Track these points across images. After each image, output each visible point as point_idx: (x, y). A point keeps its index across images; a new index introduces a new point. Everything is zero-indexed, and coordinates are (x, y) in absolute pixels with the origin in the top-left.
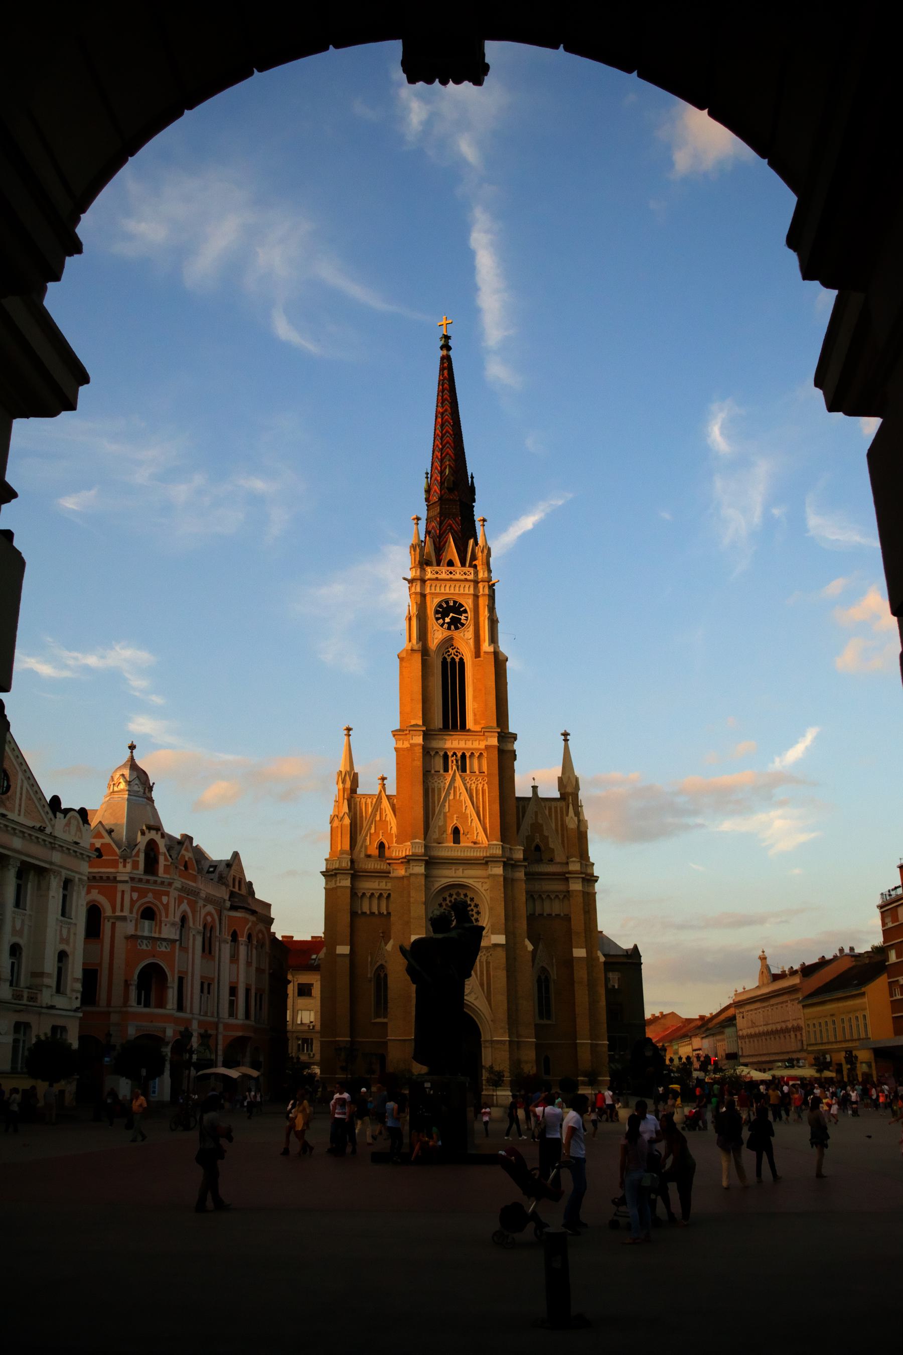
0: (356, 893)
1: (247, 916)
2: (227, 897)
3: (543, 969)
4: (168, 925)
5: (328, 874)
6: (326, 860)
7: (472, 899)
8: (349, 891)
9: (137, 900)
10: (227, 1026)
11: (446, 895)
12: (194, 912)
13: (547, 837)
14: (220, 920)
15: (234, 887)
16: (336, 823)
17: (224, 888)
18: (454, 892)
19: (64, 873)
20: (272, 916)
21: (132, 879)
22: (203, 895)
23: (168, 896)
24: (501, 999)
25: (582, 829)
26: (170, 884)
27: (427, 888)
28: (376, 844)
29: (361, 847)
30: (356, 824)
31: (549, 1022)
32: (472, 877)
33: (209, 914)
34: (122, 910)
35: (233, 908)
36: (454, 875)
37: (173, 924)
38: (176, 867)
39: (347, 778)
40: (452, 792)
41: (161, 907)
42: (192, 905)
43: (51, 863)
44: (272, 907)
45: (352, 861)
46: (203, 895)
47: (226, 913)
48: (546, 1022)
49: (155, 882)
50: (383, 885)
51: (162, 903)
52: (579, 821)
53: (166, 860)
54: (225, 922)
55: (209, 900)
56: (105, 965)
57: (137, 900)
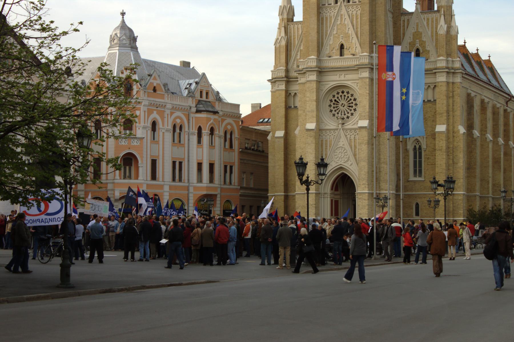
2: (194, 105)
3: (417, 141)
4: (141, 129)
5: (273, 81)
6: (272, 71)
7: (352, 95)
8: (283, 93)
10: (195, 188)
11: (335, 93)
12: (163, 118)
13: (425, 42)
14: (188, 120)
15: (201, 97)
18: (340, 91)
20: (241, 113)
23: (140, 110)
24: (364, 165)
25: (453, 33)
27: (318, 90)
29: (294, 61)
31: (420, 179)
32: (348, 79)
33: (178, 117)
35: (198, 111)
36: (338, 79)
37: (144, 128)
39: (285, 11)
40: (339, 18)
42: (161, 114)
44: (241, 107)
45: (287, 71)
46: (169, 106)
47: (192, 115)
48: (418, 179)
52: (449, 27)
54: (193, 122)
55: (174, 109)
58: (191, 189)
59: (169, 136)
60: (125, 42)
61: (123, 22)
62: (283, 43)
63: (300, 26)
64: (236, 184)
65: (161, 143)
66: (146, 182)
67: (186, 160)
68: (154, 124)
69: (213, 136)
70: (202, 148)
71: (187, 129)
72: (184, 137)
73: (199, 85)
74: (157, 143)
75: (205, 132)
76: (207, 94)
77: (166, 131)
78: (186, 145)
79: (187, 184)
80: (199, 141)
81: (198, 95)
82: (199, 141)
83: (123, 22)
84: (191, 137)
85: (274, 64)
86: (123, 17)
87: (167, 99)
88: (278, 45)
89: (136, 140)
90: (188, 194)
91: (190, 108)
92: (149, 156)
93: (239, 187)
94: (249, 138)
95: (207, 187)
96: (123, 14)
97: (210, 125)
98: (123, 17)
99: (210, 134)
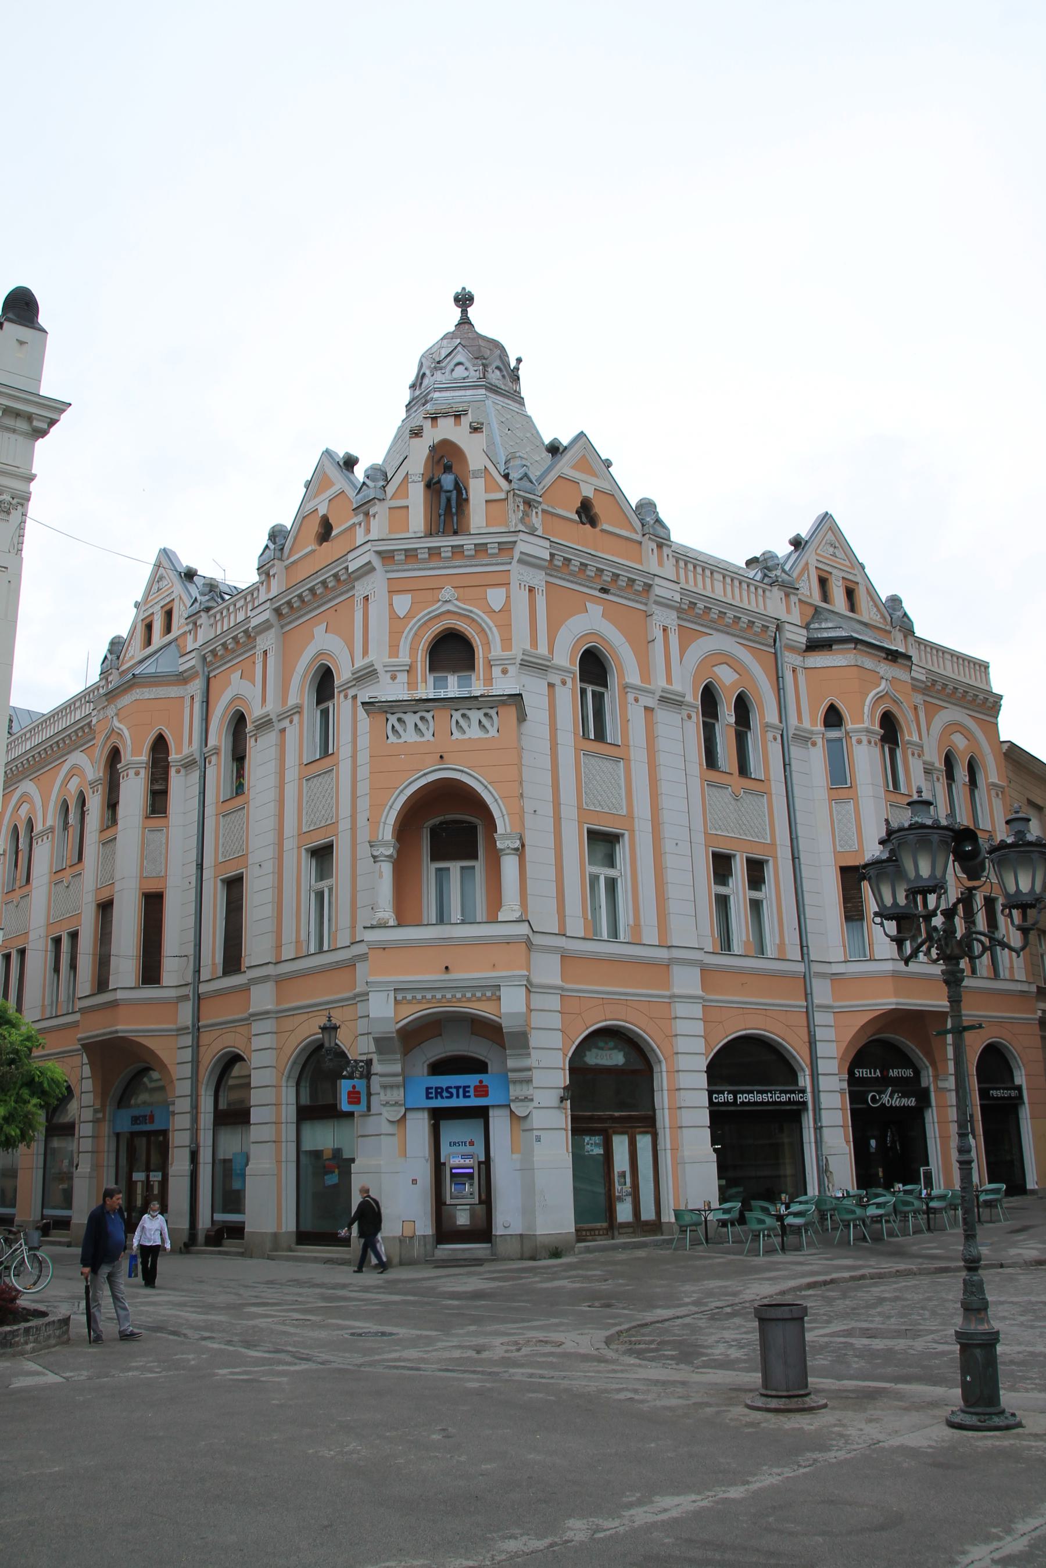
1: (868, 663)
4: (512, 670)
9: (408, 617)
17: (776, 593)
20: (996, 689)
21: (386, 556)
26: (506, 548)
34: (365, 652)
35: (815, 646)
38: (528, 503)
41: (487, 621)
44: (992, 670)
47: (791, 659)
49: (457, 551)
53: (491, 485)
56: (344, 825)
58: (822, 993)
59: (681, 735)
60: (466, 374)
61: (465, 321)
64: (1020, 975)
66: (561, 942)
67: (784, 853)
68: (594, 666)
69: (899, 753)
70: (856, 800)
73: (810, 549)
74: (620, 756)
76: (850, 593)
77: (663, 700)
78: (778, 788)
79: (801, 968)
80: (839, 775)
81: (810, 590)
82: (839, 775)
83: (465, 321)
84: (795, 751)
86: (464, 312)
87: (654, 559)
89: (475, 715)
90: (808, 1014)
91: (778, 628)
93: (1033, 989)
94: (1039, 802)
95: (895, 975)
96: (464, 300)
97: (879, 699)
98: (464, 312)
99: (884, 739)
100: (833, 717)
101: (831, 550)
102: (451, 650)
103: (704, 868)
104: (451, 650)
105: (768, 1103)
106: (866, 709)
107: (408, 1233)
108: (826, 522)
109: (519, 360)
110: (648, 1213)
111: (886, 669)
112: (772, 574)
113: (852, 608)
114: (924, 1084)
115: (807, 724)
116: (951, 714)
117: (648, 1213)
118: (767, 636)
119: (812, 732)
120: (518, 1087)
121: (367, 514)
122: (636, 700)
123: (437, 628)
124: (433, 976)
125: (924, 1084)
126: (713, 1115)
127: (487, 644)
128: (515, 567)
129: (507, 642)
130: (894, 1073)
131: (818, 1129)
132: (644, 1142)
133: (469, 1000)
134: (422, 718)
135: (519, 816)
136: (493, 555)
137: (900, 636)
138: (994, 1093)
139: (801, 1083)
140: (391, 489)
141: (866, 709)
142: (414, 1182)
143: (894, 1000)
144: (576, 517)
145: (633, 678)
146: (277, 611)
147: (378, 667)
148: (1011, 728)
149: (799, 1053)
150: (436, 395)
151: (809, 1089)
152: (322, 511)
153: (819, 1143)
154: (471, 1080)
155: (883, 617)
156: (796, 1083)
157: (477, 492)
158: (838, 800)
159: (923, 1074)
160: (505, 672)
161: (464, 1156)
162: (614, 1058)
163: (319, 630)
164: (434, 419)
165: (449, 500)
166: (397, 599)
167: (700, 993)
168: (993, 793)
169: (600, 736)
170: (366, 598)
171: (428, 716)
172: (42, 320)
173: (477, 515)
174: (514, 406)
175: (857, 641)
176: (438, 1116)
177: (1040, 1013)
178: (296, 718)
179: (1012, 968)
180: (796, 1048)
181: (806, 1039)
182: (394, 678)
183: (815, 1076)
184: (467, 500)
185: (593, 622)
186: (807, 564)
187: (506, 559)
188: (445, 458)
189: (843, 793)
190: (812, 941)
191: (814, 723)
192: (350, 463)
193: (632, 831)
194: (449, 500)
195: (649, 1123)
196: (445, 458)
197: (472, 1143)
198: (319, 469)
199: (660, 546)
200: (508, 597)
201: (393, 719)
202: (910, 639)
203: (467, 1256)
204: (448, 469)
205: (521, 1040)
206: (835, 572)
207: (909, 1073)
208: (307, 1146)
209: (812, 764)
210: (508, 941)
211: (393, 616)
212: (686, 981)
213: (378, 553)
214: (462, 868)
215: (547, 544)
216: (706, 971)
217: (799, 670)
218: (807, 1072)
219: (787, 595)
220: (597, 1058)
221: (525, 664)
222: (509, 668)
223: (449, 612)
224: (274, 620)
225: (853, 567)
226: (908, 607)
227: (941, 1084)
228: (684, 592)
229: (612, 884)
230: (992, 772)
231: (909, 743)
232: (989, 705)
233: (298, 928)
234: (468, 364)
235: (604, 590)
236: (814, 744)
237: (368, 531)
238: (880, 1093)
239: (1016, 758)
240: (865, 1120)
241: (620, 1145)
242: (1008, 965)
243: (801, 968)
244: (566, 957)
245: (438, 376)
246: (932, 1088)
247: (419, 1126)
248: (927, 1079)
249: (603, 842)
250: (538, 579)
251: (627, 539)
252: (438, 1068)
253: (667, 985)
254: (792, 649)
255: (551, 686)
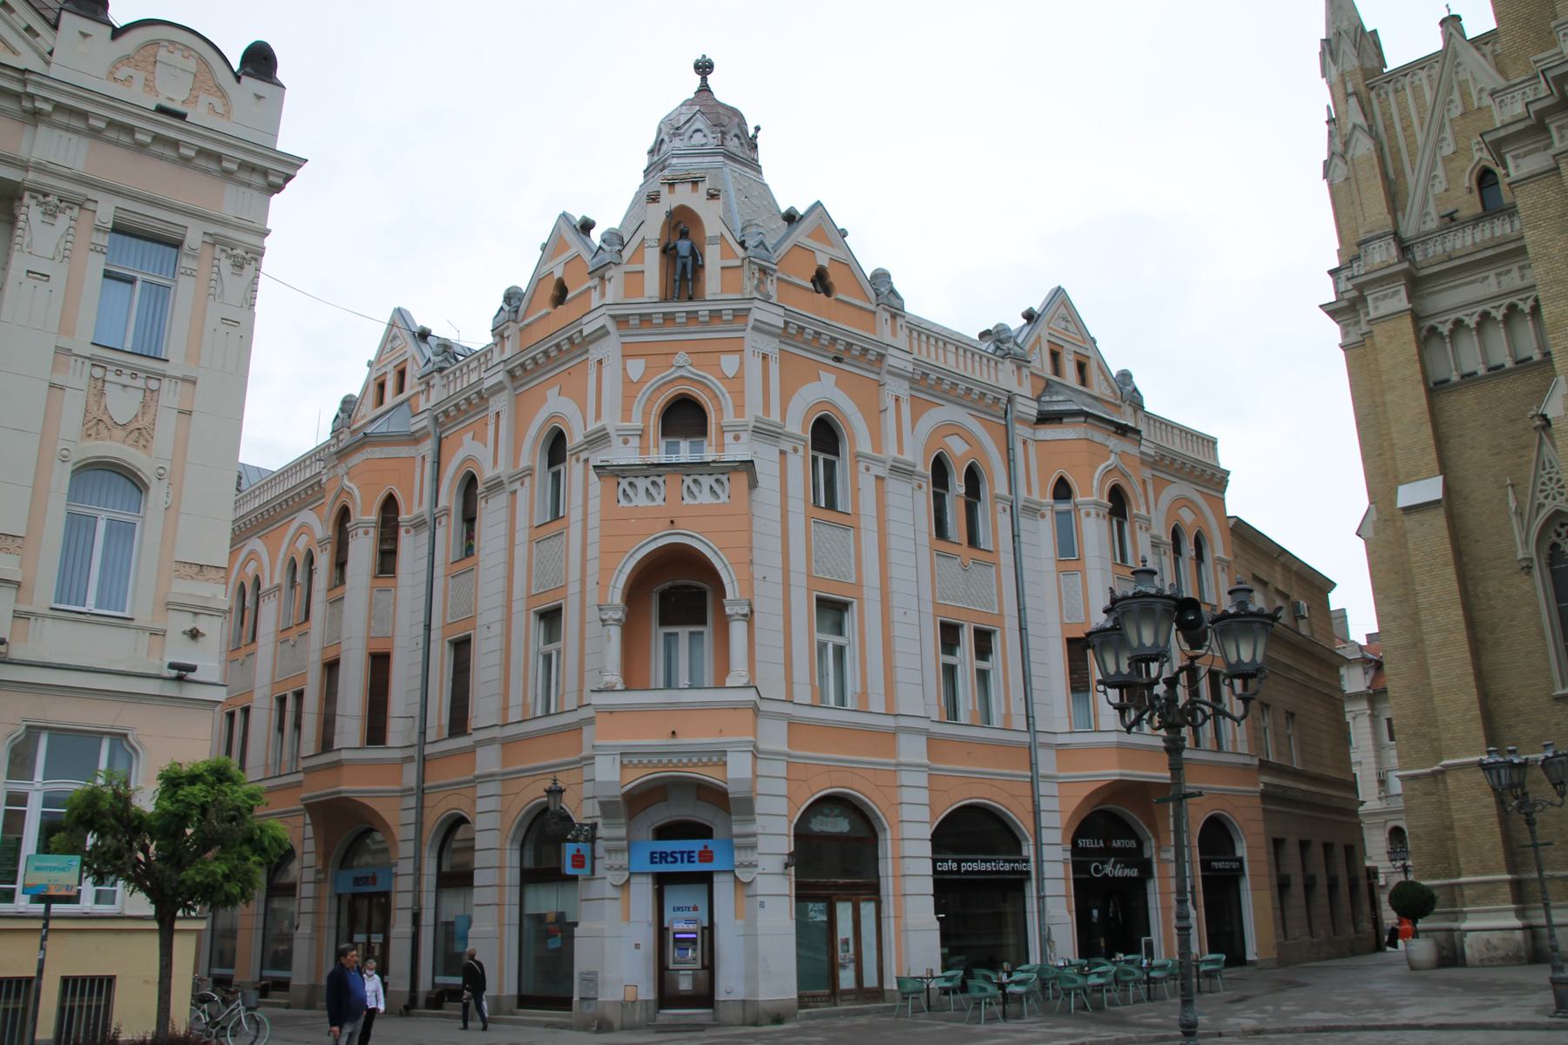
0: (1433, 330)
1: (1098, 436)
4: (744, 436)
6: (1332, 273)
9: (641, 382)
16: (1341, 170)
17: (1008, 366)
19: (107, 210)
21: (621, 321)
22: (894, 360)
26: (740, 315)
28: (1468, 180)
30: (1396, 152)
34: (598, 416)
35: (1045, 418)
38: (764, 271)
41: (720, 387)
43: (41, 168)
47: (1021, 431)
49: (692, 316)
50: (1514, 280)
51: (723, 378)
53: (727, 252)
56: (574, 588)
57: (641, 382)
58: (1047, 763)
59: (911, 505)
60: (704, 141)
61: (704, 89)
62: (1363, 146)
63: (1423, 74)
64: (1243, 748)
65: (869, 524)
66: (787, 708)
67: (1011, 624)
68: (826, 434)
69: (1127, 526)
70: (1083, 572)
71: (1002, 488)
72: (994, 524)
73: (1042, 323)
74: (850, 525)
75: (1091, 495)
76: (1081, 368)
77: (894, 469)
78: (1006, 559)
79: (1026, 738)
80: (1067, 547)
82: (1067, 547)
83: (704, 89)
84: (1025, 523)
85: (1337, 246)
86: (704, 79)
87: (887, 329)
88: (1341, 170)
89: (707, 481)
91: (1010, 400)
92: (799, 580)
93: (1256, 762)
94: (1264, 577)
95: (1120, 746)
96: (704, 68)
97: (1108, 472)
98: (704, 79)
99: (1112, 512)
100: (1062, 490)
101: (1063, 324)
102: (684, 416)
103: (932, 637)
104: (684, 416)
105: (992, 872)
106: (1095, 482)
107: (630, 997)
108: (1059, 297)
109: (757, 129)
110: (870, 981)
111: (1114, 443)
112: (1005, 347)
113: (1083, 382)
114: (1146, 855)
115: (1036, 496)
116: (1178, 489)
117: (870, 981)
118: (998, 409)
119: (1041, 504)
120: (743, 853)
121: (602, 278)
122: (868, 469)
123: (671, 392)
124: (659, 741)
125: (1146, 855)
126: (936, 883)
127: (720, 410)
128: (749, 335)
129: (739, 409)
130: (1117, 844)
131: (1041, 898)
132: (867, 909)
133: (695, 765)
134: (654, 483)
135: (748, 583)
136: (728, 322)
137: (1129, 410)
138: (1215, 864)
139: (1025, 852)
140: (627, 254)
141: (1095, 482)
142: (637, 946)
143: (1118, 771)
144: (811, 286)
145: (865, 446)
146: (511, 373)
147: (611, 430)
148: (1237, 503)
149: (1024, 825)
150: (675, 161)
151: (1032, 859)
152: (558, 274)
153: (1041, 912)
154: (696, 845)
155: (1114, 392)
156: (1019, 851)
157: (713, 259)
158: (1067, 573)
159: (1146, 845)
160: (737, 438)
161: (688, 921)
162: (840, 825)
163: (552, 393)
164: (672, 185)
165: (684, 266)
166: (631, 363)
167: (926, 761)
168: (1219, 567)
169: (831, 504)
170: (600, 362)
171: (660, 480)
172: (281, 74)
173: (712, 281)
174: (751, 174)
175: (1087, 415)
176: (663, 881)
177: (1261, 786)
178: (527, 480)
179: (1235, 740)
180: (1020, 818)
181: (1030, 808)
182: (626, 442)
183: (1038, 845)
184: (702, 266)
185: (825, 390)
186: (1039, 337)
187: (740, 326)
188: (682, 224)
189: (1071, 566)
190: (1038, 711)
191: (1043, 495)
192: (586, 226)
193: (861, 599)
194: (684, 266)
195: (872, 890)
196: (682, 224)
197: (695, 909)
198: (556, 233)
199: (894, 316)
200: (741, 363)
201: (624, 483)
202: (1140, 414)
203: (689, 1020)
204: (684, 235)
205: (746, 806)
206: (1066, 345)
207: (1132, 844)
208: (531, 909)
209: (1041, 536)
210: (735, 707)
211: (627, 381)
212: (912, 750)
213: (613, 317)
214: (691, 633)
215: (781, 312)
216: (931, 739)
217: (1030, 443)
218: (1031, 842)
219: (1019, 368)
220: (821, 825)
221: (757, 431)
222: (742, 435)
223: (682, 377)
224: (507, 382)
225: (1084, 341)
226: (1138, 381)
227: (1163, 856)
228: (917, 363)
229: (840, 652)
230: (1218, 547)
231: (1136, 516)
232: (1216, 481)
233: (525, 690)
234: (707, 131)
235: (837, 359)
236: (1043, 516)
237: (603, 295)
238: (1103, 863)
239: (1244, 536)
240: (1087, 891)
241: (844, 911)
242: (1230, 737)
243: (1026, 738)
244: (793, 724)
245: (677, 142)
246: (1154, 860)
247: (643, 890)
248: (1150, 851)
249: (832, 610)
250: (772, 346)
251: (862, 309)
252: (663, 833)
253: (893, 752)
254: (1023, 421)
255: (783, 453)
